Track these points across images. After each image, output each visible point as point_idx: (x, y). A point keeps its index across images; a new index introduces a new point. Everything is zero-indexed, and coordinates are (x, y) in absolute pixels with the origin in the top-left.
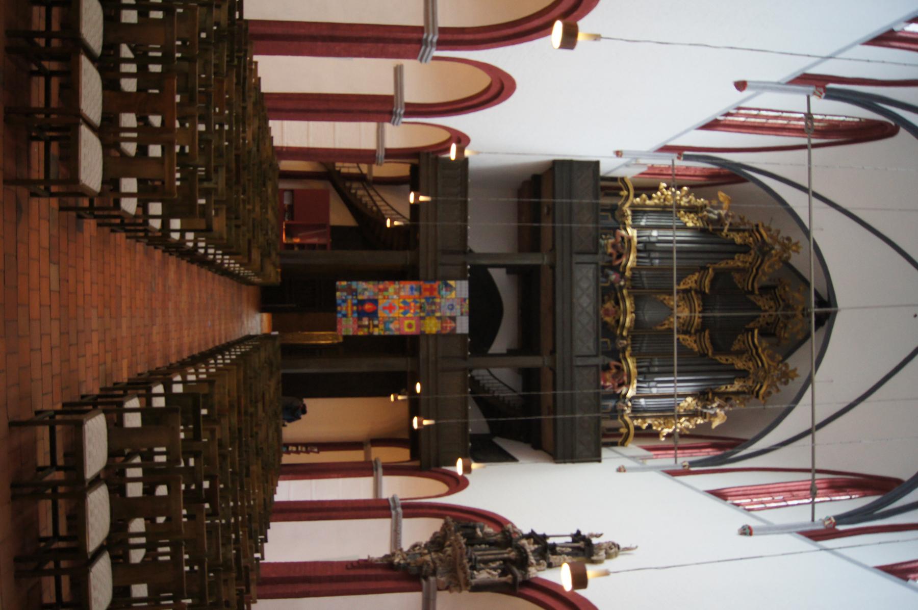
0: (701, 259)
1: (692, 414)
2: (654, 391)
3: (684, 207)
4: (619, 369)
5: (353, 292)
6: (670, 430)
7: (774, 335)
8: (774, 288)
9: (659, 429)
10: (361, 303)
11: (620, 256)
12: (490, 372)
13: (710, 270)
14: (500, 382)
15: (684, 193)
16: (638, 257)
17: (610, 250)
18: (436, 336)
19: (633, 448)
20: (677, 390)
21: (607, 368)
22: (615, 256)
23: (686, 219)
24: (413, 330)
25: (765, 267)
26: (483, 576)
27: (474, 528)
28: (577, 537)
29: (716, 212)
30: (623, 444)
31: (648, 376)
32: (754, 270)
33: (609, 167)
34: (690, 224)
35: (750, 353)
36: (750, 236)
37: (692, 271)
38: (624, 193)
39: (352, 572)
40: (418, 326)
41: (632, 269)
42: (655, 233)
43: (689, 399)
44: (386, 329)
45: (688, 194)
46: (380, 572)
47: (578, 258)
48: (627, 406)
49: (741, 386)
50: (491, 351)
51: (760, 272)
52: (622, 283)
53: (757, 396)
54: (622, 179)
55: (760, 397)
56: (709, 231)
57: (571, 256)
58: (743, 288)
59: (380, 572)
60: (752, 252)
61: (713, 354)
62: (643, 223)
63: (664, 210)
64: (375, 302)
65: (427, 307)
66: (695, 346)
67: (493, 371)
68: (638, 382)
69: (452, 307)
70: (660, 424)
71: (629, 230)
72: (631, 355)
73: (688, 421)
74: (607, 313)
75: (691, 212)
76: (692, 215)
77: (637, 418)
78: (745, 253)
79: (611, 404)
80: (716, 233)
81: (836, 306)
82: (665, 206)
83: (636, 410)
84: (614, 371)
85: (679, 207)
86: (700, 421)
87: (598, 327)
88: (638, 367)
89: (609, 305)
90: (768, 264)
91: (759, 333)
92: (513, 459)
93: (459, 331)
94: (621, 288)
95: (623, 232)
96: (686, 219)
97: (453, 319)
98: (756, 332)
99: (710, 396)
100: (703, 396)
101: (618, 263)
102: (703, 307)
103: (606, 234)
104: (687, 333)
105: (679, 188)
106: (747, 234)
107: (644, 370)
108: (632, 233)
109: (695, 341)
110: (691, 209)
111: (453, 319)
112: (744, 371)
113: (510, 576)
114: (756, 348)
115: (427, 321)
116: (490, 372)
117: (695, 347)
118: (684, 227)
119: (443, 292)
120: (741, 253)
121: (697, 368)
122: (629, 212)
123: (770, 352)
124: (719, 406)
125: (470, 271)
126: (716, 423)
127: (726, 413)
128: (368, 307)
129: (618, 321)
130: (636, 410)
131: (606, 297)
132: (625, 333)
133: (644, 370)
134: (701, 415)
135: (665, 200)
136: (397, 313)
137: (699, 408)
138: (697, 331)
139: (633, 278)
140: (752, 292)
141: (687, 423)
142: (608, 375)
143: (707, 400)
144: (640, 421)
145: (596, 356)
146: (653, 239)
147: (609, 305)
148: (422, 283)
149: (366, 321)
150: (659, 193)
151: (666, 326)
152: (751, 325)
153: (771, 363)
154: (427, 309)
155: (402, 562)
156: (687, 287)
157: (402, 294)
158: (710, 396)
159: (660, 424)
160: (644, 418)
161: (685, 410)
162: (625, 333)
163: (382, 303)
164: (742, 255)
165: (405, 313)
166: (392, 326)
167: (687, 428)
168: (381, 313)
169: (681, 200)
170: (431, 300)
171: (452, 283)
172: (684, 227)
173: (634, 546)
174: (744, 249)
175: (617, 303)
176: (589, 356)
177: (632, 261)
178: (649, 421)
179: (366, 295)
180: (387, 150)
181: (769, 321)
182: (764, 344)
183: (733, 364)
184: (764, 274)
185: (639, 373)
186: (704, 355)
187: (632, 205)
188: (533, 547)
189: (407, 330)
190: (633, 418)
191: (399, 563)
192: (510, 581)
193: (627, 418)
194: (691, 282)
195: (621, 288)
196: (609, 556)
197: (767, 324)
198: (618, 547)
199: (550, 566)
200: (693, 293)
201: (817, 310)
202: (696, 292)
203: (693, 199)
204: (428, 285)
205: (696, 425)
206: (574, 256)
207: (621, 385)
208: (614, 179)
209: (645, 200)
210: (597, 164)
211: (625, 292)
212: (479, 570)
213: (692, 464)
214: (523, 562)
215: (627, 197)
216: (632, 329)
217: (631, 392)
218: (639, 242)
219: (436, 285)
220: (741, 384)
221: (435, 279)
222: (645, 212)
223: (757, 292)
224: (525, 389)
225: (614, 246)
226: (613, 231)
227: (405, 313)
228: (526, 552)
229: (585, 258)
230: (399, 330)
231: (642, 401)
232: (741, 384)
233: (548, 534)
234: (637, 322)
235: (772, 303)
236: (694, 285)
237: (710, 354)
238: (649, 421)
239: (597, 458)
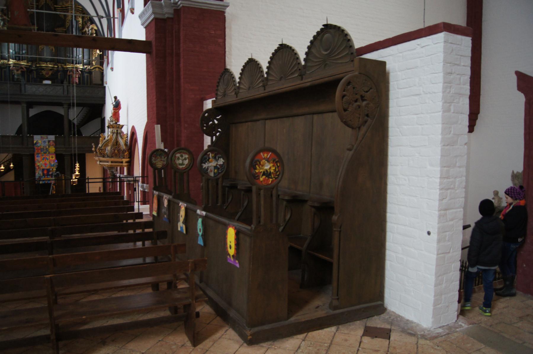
2: (80, 56)
5: (40, 177)
10: (43, 174)
11: (22, 68)
16: (22, 60)
17: (19, 72)
18: (56, 148)
24: (54, 156)
40: (52, 154)
41: (28, 63)
42: (11, 51)
44: (54, 166)
64: (43, 170)
65: (45, 151)
68: (76, 64)
69: (45, 142)
72: (65, 65)
74: (47, 74)
77: (92, 63)
83: (89, 63)
91: (56, 5)
93: (54, 139)
94: (36, 67)
97: (49, 141)
101: (25, 69)
108: (11, 62)
111: (49, 141)
114: (62, 7)
115: (50, 151)
119: (39, 145)
124: (88, 28)
125: (30, 135)
128: (45, 172)
129: (51, 70)
131: (41, 74)
132: (56, 67)
136: (47, 162)
145: (63, 86)
146: (14, 52)
147: (44, 73)
148: (35, 153)
149: (50, 173)
154: (46, 151)
157: (40, 160)
162: (56, 67)
163: (44, 167)
165: (47, 159)
166: (53, 164)
168: (48, 167)
170: (42, 150)
171: (35, 142)
175: (43, 69)
176: (64, 89)
179: (41, 173)
185: (73, 63)
189: (54, 158)
190: (92, 65)
193: (92, 68)
195: (36, 67)
204: (36, 151)
207: (78, 71)
211: (38, 65)
217: (81, 66)
218: (15, 59)
219: (36, 148)
221: (34, 148)
225: (17, 70)
226: (11, 71)
227: (47, 159)
229: (23, 89)
230: (54, 161)
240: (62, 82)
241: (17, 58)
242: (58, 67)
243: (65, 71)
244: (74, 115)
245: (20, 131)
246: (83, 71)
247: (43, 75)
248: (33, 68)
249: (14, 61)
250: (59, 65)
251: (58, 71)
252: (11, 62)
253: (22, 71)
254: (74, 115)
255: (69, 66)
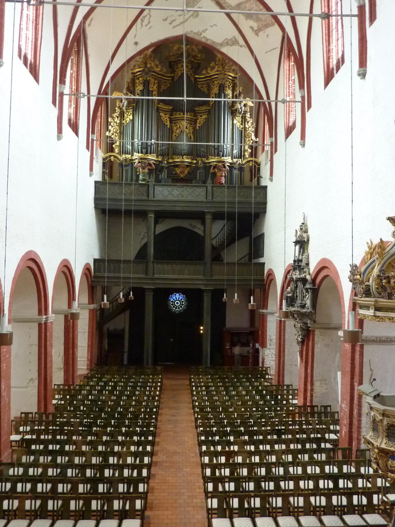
0: (152, 114)
1: (244, 120)
3: (121, 120)
4: (215, 167)
6: (253, 134)
7: (199, 65)
8: (170, 62)
9: (252, 141)
11: (150, 165)
12: (214, 238)
13: (159, 106)
14: (220, 232)
15: (112, 121)
16: (151, 154)
17: (146, 170)
19: (262, 158)
20: (230, 126)
21: (214, 174)
22: (150, 167)
23: (128, 119)
25: (157, 70)
26: (308, 302)
27: (287, 297)
28: (296, 243)
29: (123, 101)
30: (259, 165)
31: (220, 150)
32: (159, 76)
33: (98, 176)
34: (131, 117)
35: (210, 81)
36: (139, 79)
37: (159, 117)
38: (112, 158)
39: (304, 361)
41: (157, 157)
43: (235, 122)
45: (113, 118)
46: (305, 348)
47: (151, 197)
48: (237, 162)
49: (229, 88)
50: (203, 235)
51: (161, 73)
52: (165, 162)
53: (236, 78)
54: (104, 159)
55: (236, 76)
56: (134, 105)
57: (150, 201)
58: (170, 83)
59: (305, 348)
60: (148, 79)
61: (209, 106)
62: (130, 147)
63: (122, 134)
66: (204, 117)
67: (213, 236)
68: (223, 156)
70: (249, 141)
71: (134, 158)
72: (208, 159)
73: (248, 122)
75: (124, 116)
76: (125, 115)
77: (244, 155)
78: (149, 83)
79: (236, 172)
80: (137, 101)
81: (182, 36)
82: (120, 132)
83: (241, 156)
84: (216, 170)
85: (121, 123)
86: (248, 115)
87: (191, 186)
88: (214, 156)
89: (178, 171)
90: (155, 69)
92: (262, 236)
94: (168, 163)
95: (137, 161)
96: (128, 119)
98: (196, 76)
99: (233, 109)
100: (234, 113)
102: (181, 84)
103: (137, 172)
104: (196, 122)
105: (108, 124)
106: (137, 81)
107: (216, 152)
108: (136, 156)
109: (201, 116)
110: (122, 115)
112: (219, 87)
113: (309, 290)
116: (214, 238)
117: (205, 116)
118: (133, 121)
120: (149, 86)
121: (216, 118)
122: (124, 156)
123: (209, 69)
124: (240, 104)
126: (250, 104)
127: (245, 98)
129: (187, 166)
130: (241, 156)
133: (216, 152)
134: (245, 114)
135: (116, 133)
137: (241, 116)
138: (195, 116)
139: (162, 155)
140: (173, 78)
141: (249, 124)
142: (219, 174)
143: (236, 110)
144: (246, 153)
145: (207, 187)
146: (140, 144)
147: (178, 171)
150: (112, 136)
151: (191, 135)
152: (192, 79)
153: (216, 69)
155: (301, 337)
156: (168, 120)
158: (233, 109)
159: (249, 141)
160: (245, 151)
161: (242, 124)
164: (150, 85)
167: (252, 123)
169: (116, 123)
172: (133, 121)
173: (303, 214)
174: (146, 84)
175: (177, 166)
177: (152, 157)
178: (247, 147)
180: (89, 304)
181: (191, 67)
182: (204, 72)
183: (215, 94)
184: (161, 70)
185: (218, 155)
186: (209, 112)
187: (119, 153)
188: (298, 273)
191: (301, 338)
192: (311, 291)
193: (244, 162)
194: (165, 118)
195: (168, 163)
196: (306, 232)
197: (192, 69)
198: (303, 224)
199: (308, 264)
200: (172, 117)
201: (185, 97)
202: (171, 115)
203: (115, 114)
205: (250, 118)
206: (150, 199)
207: (225, 167)
208: (104, 164)
209: (117, 146)
210: (96, 182)
212: (306, 304)
213: (271, 136)
214: (304, 281)
215: (115, 157)
216: (192, 157)
217: (228, 160)
218: (142, 153)
220: (227, 89)
222: (123, 145)
223: (173, 75)
224: (223, 219)
228: (299, 278)
231: (235, 152)
232: (227, 89)
233: (293, 259)
234: (187, 155)
235: (180, 66)
236: (168, 116)
237: (209, 108)
238: (247, 147)
239: (266, 187)
240: (204, 182)
241: (144, 151)
242: (197, 163)
243: (207, 167)
244: (216, 231)
245: (142, 254)
246: (232, 166)
247: (176, 174)
248: (163, 165)
249: (140, 155)
250: (199, 159)
251: (197, 168)
252: (136, 156)
253: (149, 169)
254: (216, 231)
255: (213, 160)
